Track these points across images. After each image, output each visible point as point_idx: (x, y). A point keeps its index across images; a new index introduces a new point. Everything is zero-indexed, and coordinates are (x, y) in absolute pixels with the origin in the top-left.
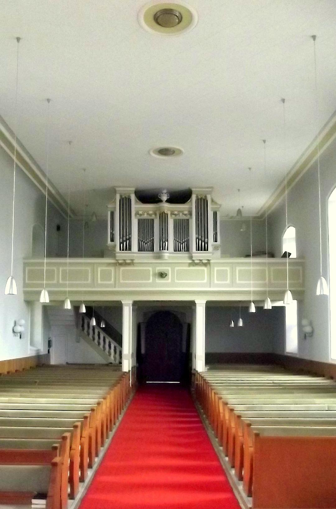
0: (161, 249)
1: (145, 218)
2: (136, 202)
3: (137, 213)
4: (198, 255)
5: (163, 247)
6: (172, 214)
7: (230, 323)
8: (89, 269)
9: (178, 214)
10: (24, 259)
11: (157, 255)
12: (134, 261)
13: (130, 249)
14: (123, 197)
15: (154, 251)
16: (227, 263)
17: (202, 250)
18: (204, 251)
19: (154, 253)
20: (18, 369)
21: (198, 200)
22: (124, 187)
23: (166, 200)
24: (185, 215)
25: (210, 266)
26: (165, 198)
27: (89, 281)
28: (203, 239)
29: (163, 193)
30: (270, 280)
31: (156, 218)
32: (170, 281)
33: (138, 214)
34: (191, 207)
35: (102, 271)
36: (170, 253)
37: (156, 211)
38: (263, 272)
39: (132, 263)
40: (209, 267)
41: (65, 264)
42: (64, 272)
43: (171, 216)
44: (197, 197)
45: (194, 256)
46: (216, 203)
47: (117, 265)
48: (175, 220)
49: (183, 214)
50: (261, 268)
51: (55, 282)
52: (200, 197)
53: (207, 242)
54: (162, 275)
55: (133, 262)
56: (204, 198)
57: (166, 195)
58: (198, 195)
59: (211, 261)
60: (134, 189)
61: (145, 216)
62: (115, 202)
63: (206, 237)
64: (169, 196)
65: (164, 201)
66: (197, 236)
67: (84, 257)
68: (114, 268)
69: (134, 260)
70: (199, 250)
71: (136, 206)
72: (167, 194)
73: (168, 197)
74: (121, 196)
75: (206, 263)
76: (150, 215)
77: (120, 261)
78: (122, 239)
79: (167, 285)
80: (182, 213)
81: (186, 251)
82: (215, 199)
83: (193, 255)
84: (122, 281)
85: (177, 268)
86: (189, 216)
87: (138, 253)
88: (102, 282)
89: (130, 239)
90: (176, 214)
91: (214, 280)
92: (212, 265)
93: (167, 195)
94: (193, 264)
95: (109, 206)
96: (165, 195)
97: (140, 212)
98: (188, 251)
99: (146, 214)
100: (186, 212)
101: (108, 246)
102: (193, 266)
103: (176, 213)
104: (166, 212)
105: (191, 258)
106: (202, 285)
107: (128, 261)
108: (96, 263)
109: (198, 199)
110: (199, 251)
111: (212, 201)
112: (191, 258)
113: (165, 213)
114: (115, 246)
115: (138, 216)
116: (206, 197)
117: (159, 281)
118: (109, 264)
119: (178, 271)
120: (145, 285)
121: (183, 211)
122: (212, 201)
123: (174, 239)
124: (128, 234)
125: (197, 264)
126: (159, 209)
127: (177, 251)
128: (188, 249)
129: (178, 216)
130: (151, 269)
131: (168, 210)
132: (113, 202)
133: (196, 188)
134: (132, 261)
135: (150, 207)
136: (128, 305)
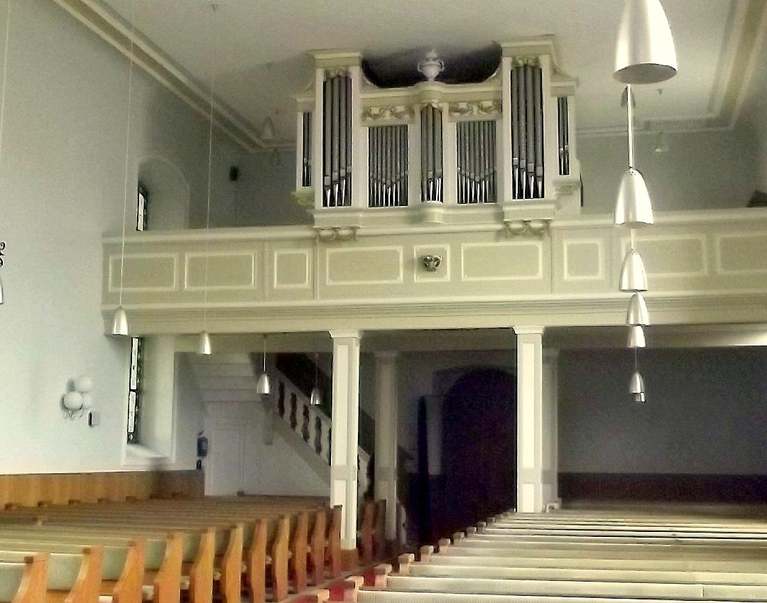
2: (364, 84)
3: (366, 113)
4: (517, 210)
5: (431, 192)
6: (454, 109)
7: (628, 381)
8: (252, 254)
9: (469, 110)
10: (105, 235)
11: (416, 213)
12: (359, 232)
13: (348, 201)
14: (332, 75)
15: (407, 205)
16: (595, 228)
17: (528, 196)
19: (409, 209)
20: (77, 497)
21: (516, 71)
22: (332, 50)
24: (486, 110)
25: (551, 237)
26: (432, 70)
27: (253, 284)
29: (428, 60)
30: (712, 266)
31: (413, 122)
32: (448, 277)
33: (370, 116)
34: (499, 89)
35: (281, 258)
36: (449, 208)
38: (693, 248)
39: (353, 237)
40: (549, 239)
41: (200, 245)
42: (196, 265)
43: (450, 115)
44: (514, 63)
45: (508, 212)
46: (564, 77)
47: (317, 241)
48: (461, 124)
49: (481, 108)
50: (688, 237)
51: (174, 287)
52: (521, 63)
54: (428, 264)
56: (533, 64)
57: (437, 63)
58: (517, 59)
59: (553, 225)
60: (357, 54)
61: (388, 119)
62: (313, 88)
67: (210, 227)
68: (311, 250)
70: (520, 196)
71: (362, 95)
74: (327, 73)
75: (542, 229)
76: (398, 115)
77: (324, 233)
78: (336, 174)
79: (440, 289)
80: (479, 107)
82: (566, 68)
83: (506, 209)
84: (329, 282)
85: (464, 246)
86: (494, 113)
87: (366, 211)
88: (194, 289)
89: (348, 176)
90: (462, 109)
91: (562, 275)
92: (555, 232)
94: (507, 232)
95: (300, 100)
97: (375, 111)
99: (388, 113)
100: (487, 104)
101: (297, 196)
102: (507, 237)
103: (463, 106)
104: (435, 106)
105: (500, 216)
106: (591, 286)
107: (344, 232)
108: (269, 240)
110: (530, 198)
111: (555, 71)
112: (500, 216)
113: (433, 108)
114: (311, 198)
115: (369, 119)
116: (537, 61)
117: (420, 278)
118: (299, 242)
119: (468, 252)
120: (391, 290)
121: (478, 103)
122: (555, 71)
123: (460, 173)
124: (343, 164)
125: (515, 233)
126: (419, 98)
127: (466, 202)
128: (492, 195)
130: (400, 250)
133: (513, 40)
135: (397, 95)
136: (345, 341)
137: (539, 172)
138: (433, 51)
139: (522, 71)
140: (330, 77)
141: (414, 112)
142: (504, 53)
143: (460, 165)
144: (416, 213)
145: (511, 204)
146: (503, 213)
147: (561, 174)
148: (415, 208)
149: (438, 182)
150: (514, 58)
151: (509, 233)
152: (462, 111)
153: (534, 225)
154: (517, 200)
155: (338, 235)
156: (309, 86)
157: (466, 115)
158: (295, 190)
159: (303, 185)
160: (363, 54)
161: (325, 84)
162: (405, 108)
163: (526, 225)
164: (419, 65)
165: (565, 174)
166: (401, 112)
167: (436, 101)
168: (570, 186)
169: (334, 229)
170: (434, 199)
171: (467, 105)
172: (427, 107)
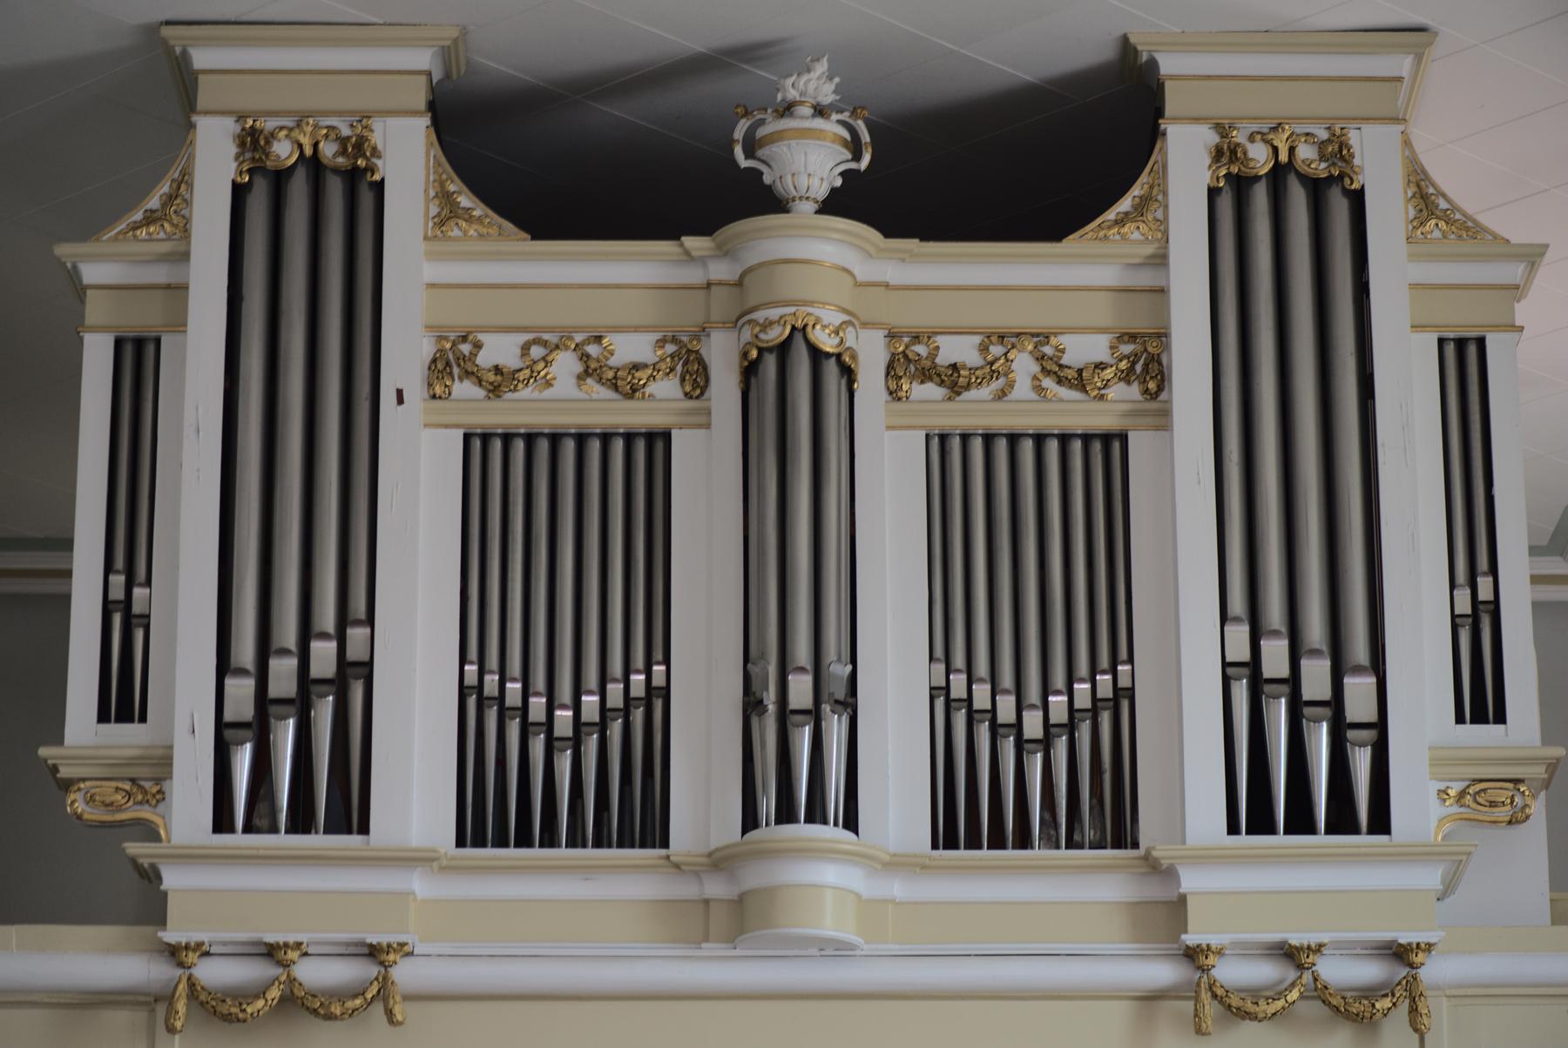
0: (768, 804)
1: (545, 420)
2: (448, 213)
9: (992, 371)
12: (405, 974)
14: (283, 151)
17: (1301, 822)
18: (1330, 830)
23: (822, 192)
24: (1079, 380)
28: (1316, 679)
29: (787, 109)
34: (1146, 278)
36: (897, 864)
37: (702, 332)
43: (894, 394)
44: (1226, 152)
49: (1053, 368)
52: (1259, 157)
53: (1371, 715)
55: (385, 983)
56: (1321, 169)
59: (1433, 971)
60: (423, 59)
63: (1359, 650)
64: (866, 137)
65: (810, 207)
66: (1240, 650)
69: (404, 950)
70: (1261, 823)
72: (835, 117)
73: (857, 157)
75: (1369, 993)
76: (626, 383)
77: (214, 973)
80: (1041, 358)
81: (1098, 845)
83: (1191, 881)
86: (1124, 394)
92: (1438, 1011)
93: (847, 136)
95: (92, 273)
96: (819, 123)
97: (499, 351)
98: (1118, 844)
99: (565, 365)
100: (1083, 349)
101: (65, 772)
103: (958, 350)
104: (827, 343)
107: (314, 973)
109: (1241, 185)
113: (817, 355)
115: (464, 389)
116: (1338, 150)
121: (1043, 337)
124: (326, 617)
129: (985, 392)
131: (854, 320)
132: (150, 219)
134: (373, 970)
137: (1359, 704)
138: (822, 67)
139: (1260, 198)
140: (269, 164)
141: (704, 368)
142: (1171, 105)
143: (940, 651)
144: (716, 888)
145: (1209, 858)
146: (1182, 900)
147: (1460, 719)
148: (720, 862)
149: (835, 729)
150: (1222, 129)
151: (1210, 1008)
152: (954, 380)
153: (1337, 971)
154: (1244, 840)
155: (292, 981)
156: (154, 202)
157: (973, 394)
158: (58, 738)
159: (103, 717)
160: (448, 54)
161: (239, 193)
162: (661, 343)
163: (1300, 967)
164: (739, 133)
165: (1479, 717)
166: (636, 367)
167: (834, 318)
168: (1517, 781)
169: (271, 952)
170: (816, 814)
171: (984, 349)
172: (783, 349)
